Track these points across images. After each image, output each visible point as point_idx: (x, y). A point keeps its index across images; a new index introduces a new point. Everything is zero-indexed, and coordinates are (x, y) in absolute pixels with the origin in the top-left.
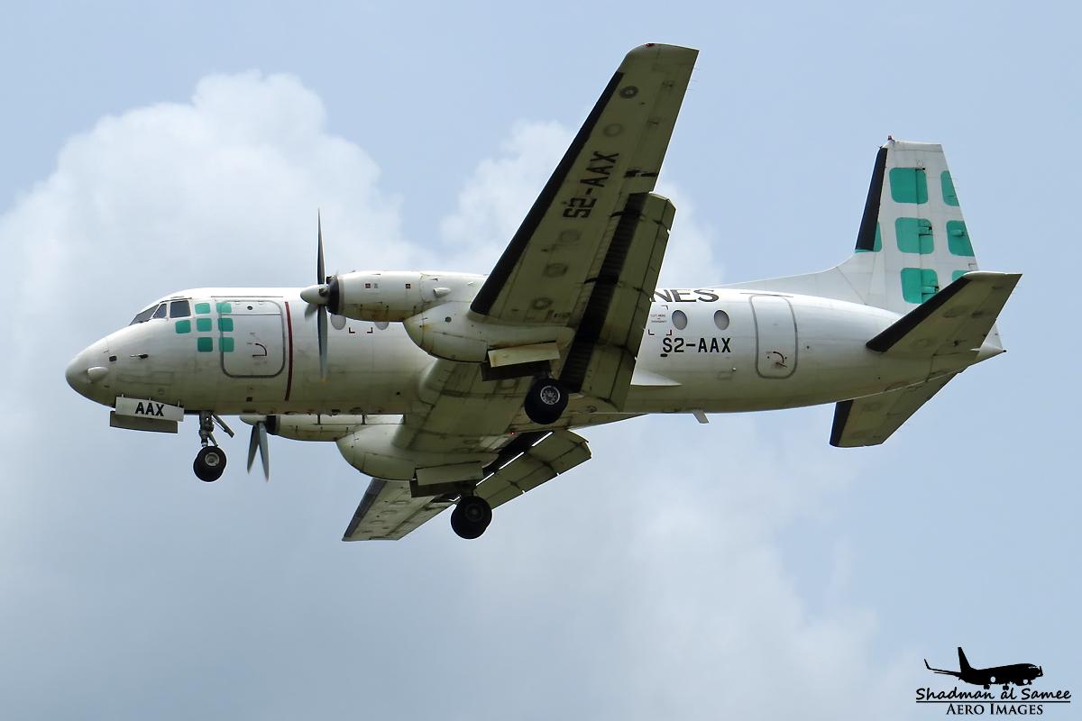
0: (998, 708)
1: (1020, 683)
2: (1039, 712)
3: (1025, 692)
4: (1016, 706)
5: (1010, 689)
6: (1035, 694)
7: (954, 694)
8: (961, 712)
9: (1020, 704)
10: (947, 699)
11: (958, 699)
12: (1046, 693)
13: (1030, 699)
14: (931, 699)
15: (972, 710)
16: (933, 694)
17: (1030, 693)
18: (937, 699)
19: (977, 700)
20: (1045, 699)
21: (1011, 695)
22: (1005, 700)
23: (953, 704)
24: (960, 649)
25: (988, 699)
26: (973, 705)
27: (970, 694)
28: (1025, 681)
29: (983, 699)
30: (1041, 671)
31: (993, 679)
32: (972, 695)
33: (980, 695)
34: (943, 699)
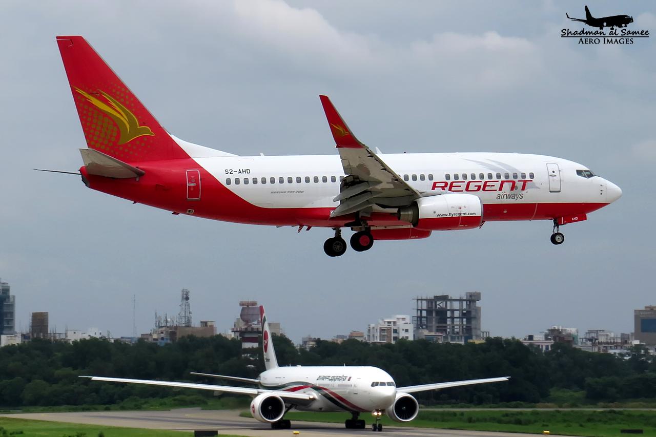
0: (608, 40)
1: (620, 26)
2: (631, 42)
3: (623, 31)
4: (618, 39)
5: (615, 29)
6: (629, 32)
7: (583, 33)
8: (587, 42)
9: (620, 38)
10: (579, 35)
11: (585, 35)
12: (635, 32)
13: (626, 35)
14: (570, 35)
15: (593, 42)
16: (571, 32)
17: (626, 32)
18: (573, 35)
19: (596, 36)
20: (635, 35)
21: (615, 33)
22: (612, 35)
23: (582, 38)
24: (586, 7)
25: (602, 35)
26: (594, 39)
27: (592, 32)
28: (623, 25)
29: (599, 35)
30: (632, 19)
31: (605, 24)
32: (593, 33)
33: (597, 33)
34: (576, 35)
